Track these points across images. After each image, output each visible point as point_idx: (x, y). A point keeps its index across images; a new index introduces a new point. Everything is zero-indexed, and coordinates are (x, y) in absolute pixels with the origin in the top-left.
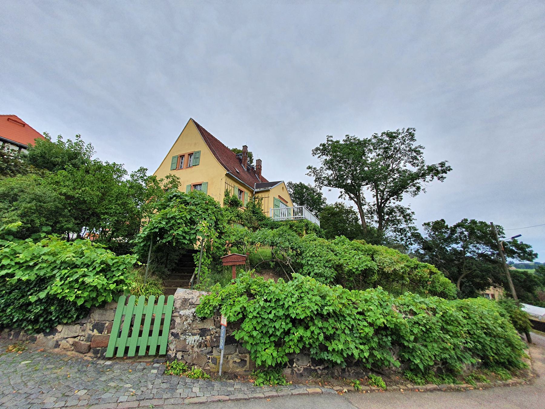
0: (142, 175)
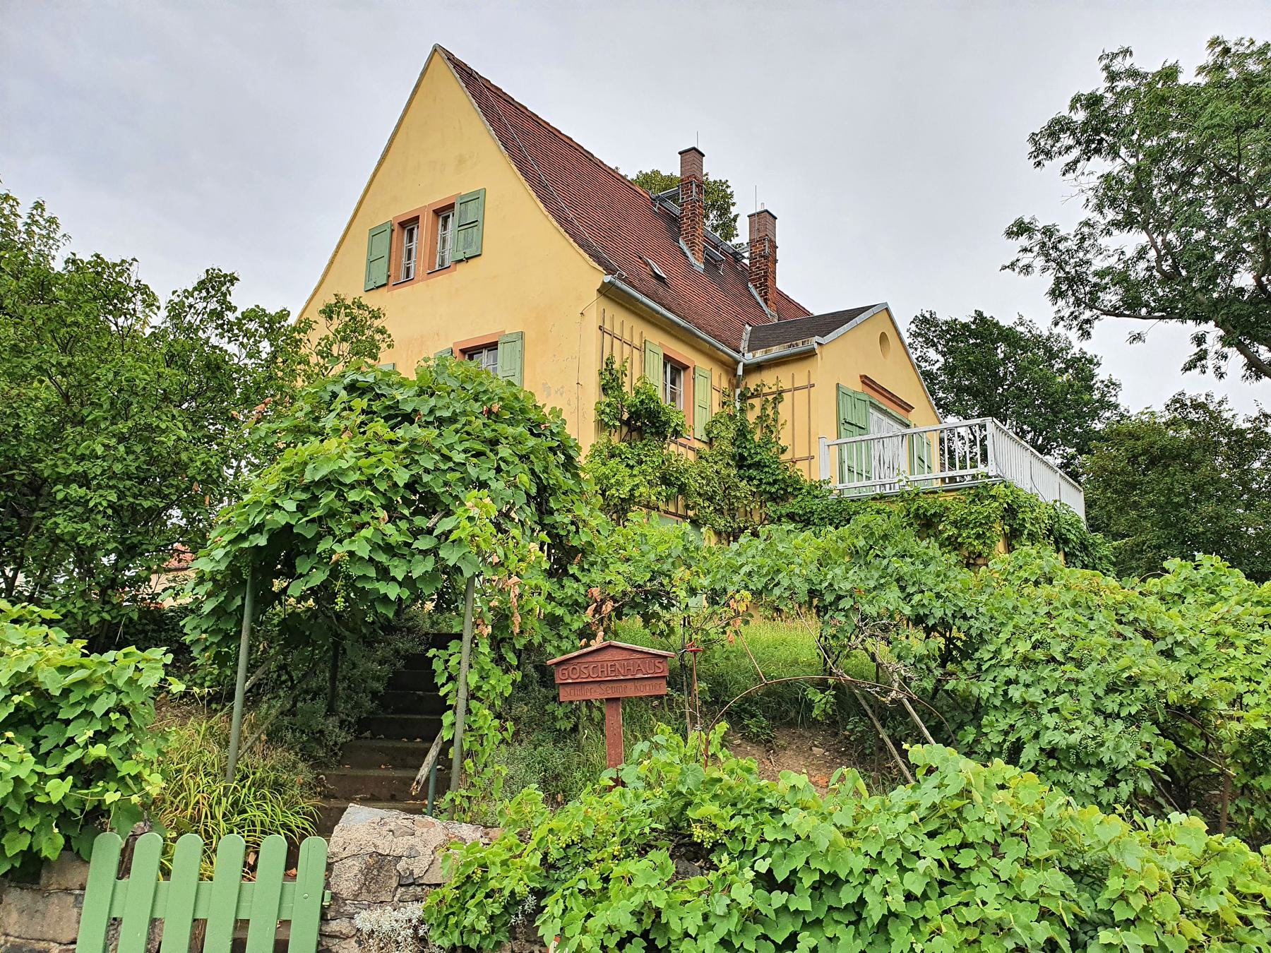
0: (213, 305)
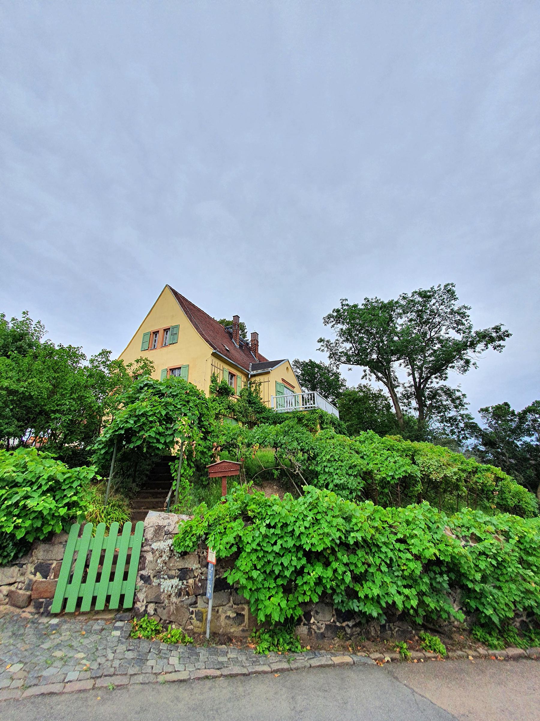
0: (104, 359)
